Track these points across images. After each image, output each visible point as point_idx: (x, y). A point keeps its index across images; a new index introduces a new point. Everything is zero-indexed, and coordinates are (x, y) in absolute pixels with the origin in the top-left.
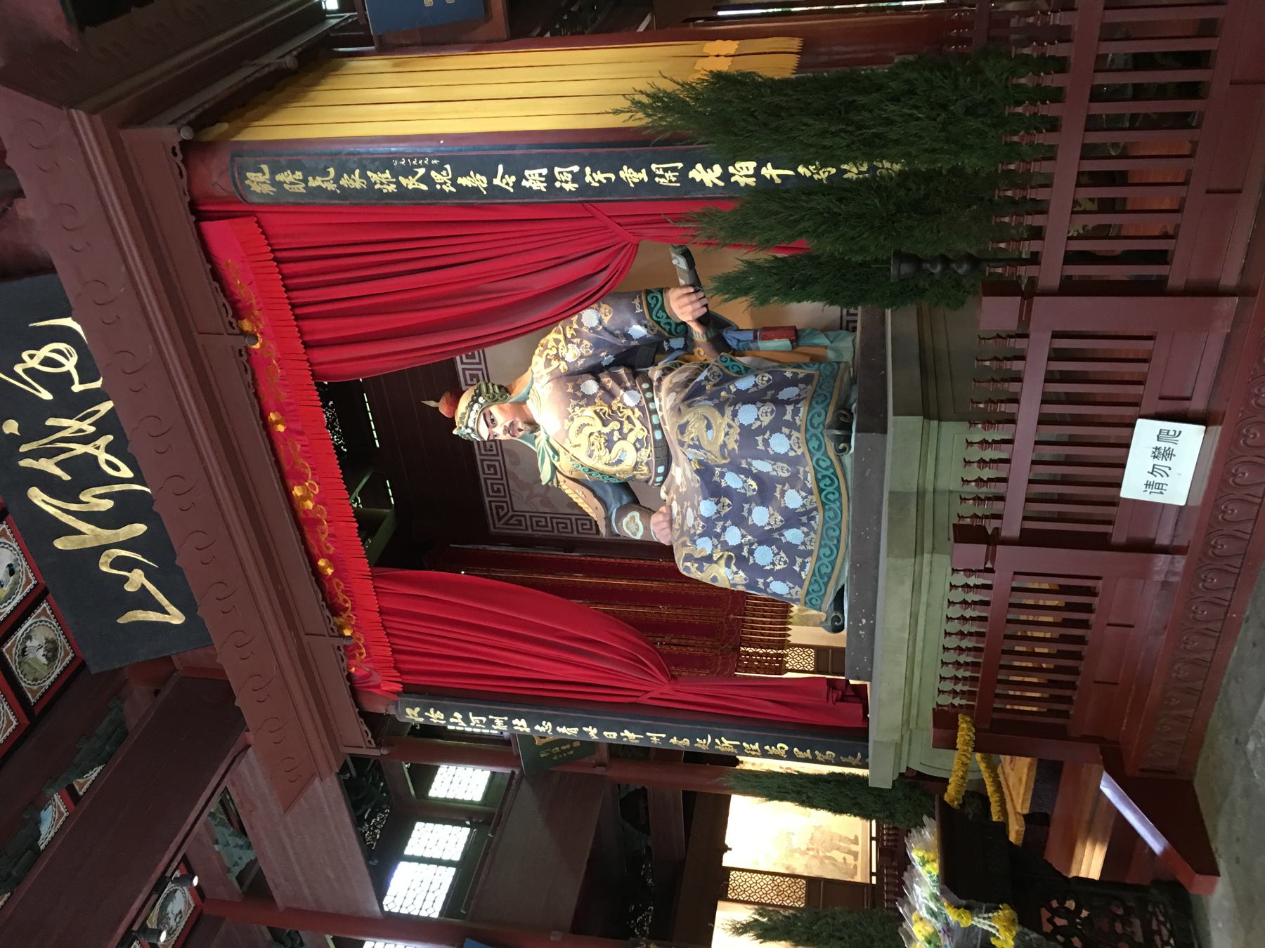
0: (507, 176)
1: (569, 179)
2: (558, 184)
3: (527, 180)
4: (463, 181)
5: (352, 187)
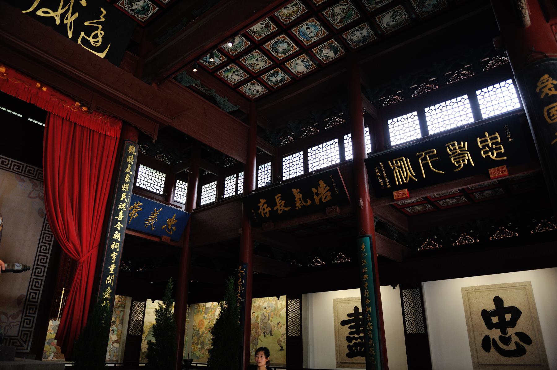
0: (120, 227)
1: (115, 247)
2: (114, 243)
3: (118, 233)
4: (121, 212)
5: (126, 177)
